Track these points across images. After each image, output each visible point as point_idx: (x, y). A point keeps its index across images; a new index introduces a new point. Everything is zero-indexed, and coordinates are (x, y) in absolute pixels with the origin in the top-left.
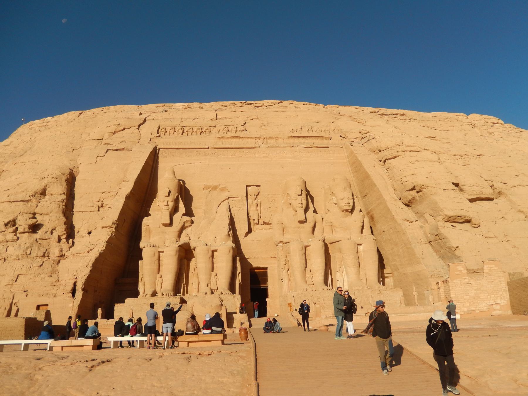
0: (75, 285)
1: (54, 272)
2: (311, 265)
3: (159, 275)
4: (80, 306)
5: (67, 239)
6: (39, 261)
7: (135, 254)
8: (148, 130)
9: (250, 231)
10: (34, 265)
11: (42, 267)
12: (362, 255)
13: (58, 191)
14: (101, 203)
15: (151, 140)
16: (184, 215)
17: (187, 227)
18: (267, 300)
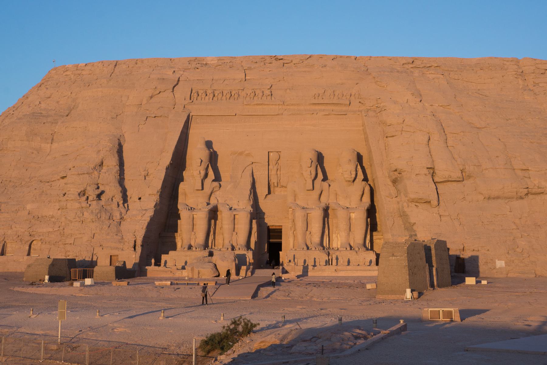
1: (119, 231)
3: (193, 233)
4: (141, 257)
5: (123, 204)
8: (182, 92)
9: (269, 192)
12: (353, 222)
13: (112, 162)
16: (213, 181)
17: (216, 191)
18: (280, 252)
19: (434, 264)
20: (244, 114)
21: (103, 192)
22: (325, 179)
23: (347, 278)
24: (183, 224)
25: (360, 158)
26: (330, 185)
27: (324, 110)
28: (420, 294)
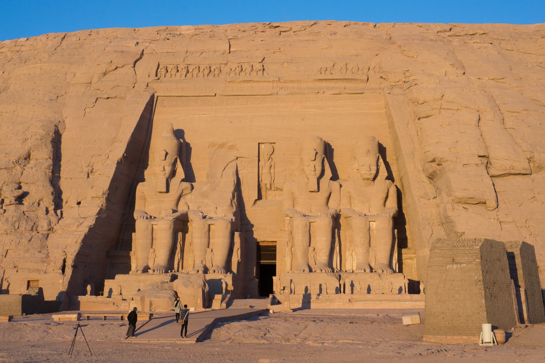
0: (64, 261)
1: (43, 247)
2: (316, 243)
3: (152, 250)
4: (70, 283)
5: (55, 210)
6: (28, 235)
7: (128, 225)
8: (146, 68)
9: (260, 197)
10: (23, 240)
11: (31, 242)
12: (374, 234)
13: (43, 156)
14: (90, 168)
15: (148, 86)
16: (183, 180)
17: (186, 194)
18: (274, 278)
19: (521, 283)
20: (226, 94)
21: (25, 194)
22: (335, 177)
23: (368, 311)
24: (139, 238)
25: (382, 150)
26: (341, 186)
27: (333, 88)
28: (508, 336)
